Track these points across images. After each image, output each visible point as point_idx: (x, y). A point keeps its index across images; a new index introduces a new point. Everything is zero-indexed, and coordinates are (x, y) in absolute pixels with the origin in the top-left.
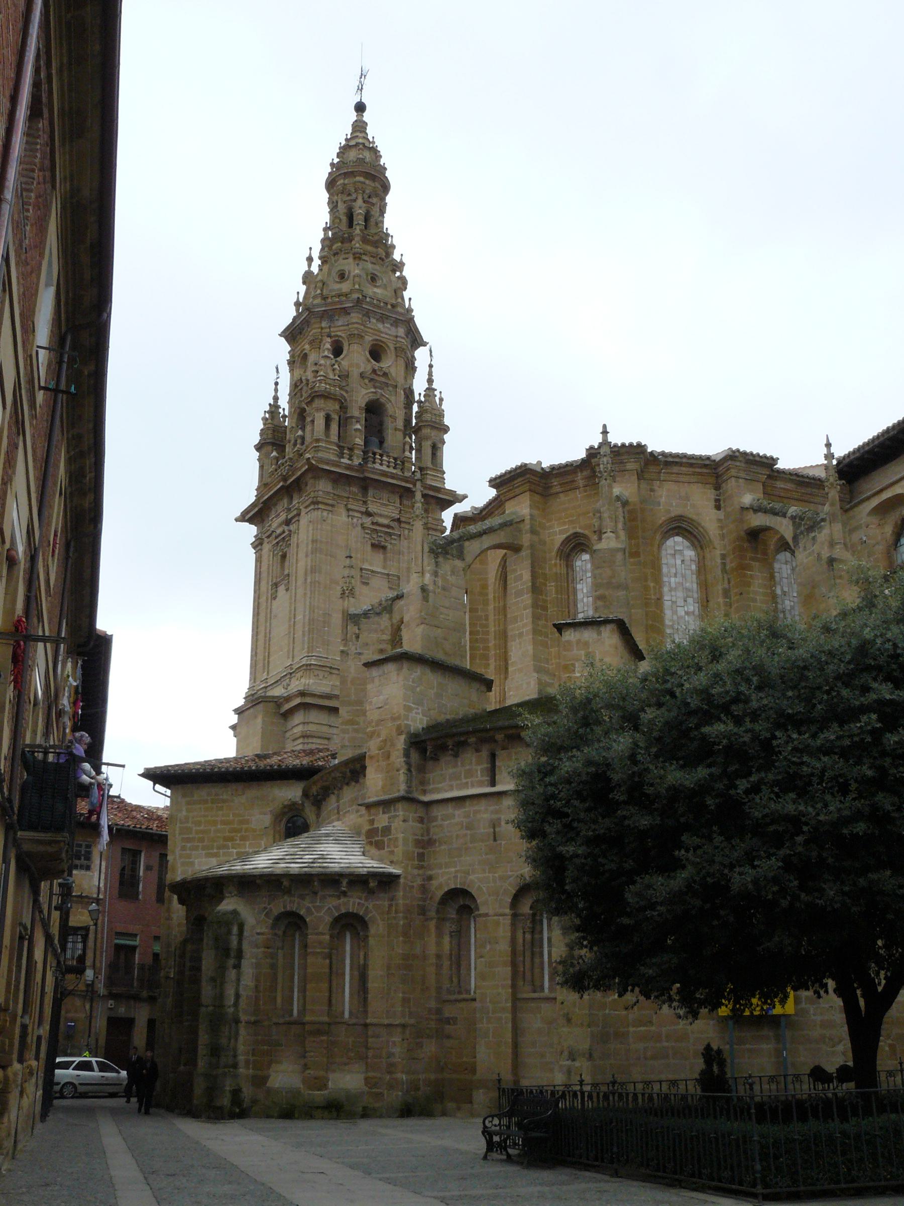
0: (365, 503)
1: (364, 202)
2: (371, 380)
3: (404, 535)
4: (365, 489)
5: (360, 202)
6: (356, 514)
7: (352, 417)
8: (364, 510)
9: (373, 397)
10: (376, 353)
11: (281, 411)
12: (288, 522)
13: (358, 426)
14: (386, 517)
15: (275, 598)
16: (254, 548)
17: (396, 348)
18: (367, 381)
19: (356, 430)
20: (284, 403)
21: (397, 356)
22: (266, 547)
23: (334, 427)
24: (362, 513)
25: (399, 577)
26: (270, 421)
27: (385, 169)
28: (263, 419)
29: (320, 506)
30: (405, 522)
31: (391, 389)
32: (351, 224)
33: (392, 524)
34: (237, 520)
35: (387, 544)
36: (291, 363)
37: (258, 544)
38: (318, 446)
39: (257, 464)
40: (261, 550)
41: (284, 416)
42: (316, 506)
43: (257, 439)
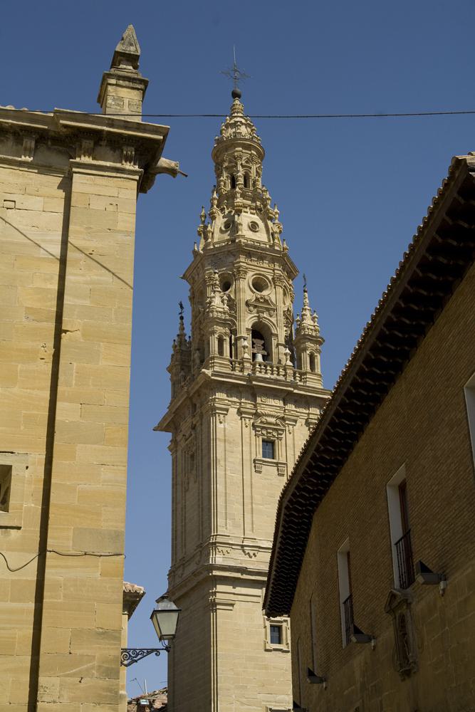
2: (255, 307)
5: (240, 168)
7: (241, 338)
8: (254, 411)
10: (258, 285)
11: (187, 338)
12: (194, 428)
13: (246, 343)
15: (187, 490)
16: (171, 451)
18: (252, 308)
19: (244, 347)
20: (188, 332)
21: (275, 286)
22: (180, 448)
23: (226, 347)
24: (252, 414)
26: (178, 348)
28: (173, 347)
30: (290, 420)
32: (234, 186)
34: (154, 430)
36: (192, 298)
38: (213, 363)
39: (170, 384)
40: (176, 451)
41: (190, 343)
43: (168, 362)
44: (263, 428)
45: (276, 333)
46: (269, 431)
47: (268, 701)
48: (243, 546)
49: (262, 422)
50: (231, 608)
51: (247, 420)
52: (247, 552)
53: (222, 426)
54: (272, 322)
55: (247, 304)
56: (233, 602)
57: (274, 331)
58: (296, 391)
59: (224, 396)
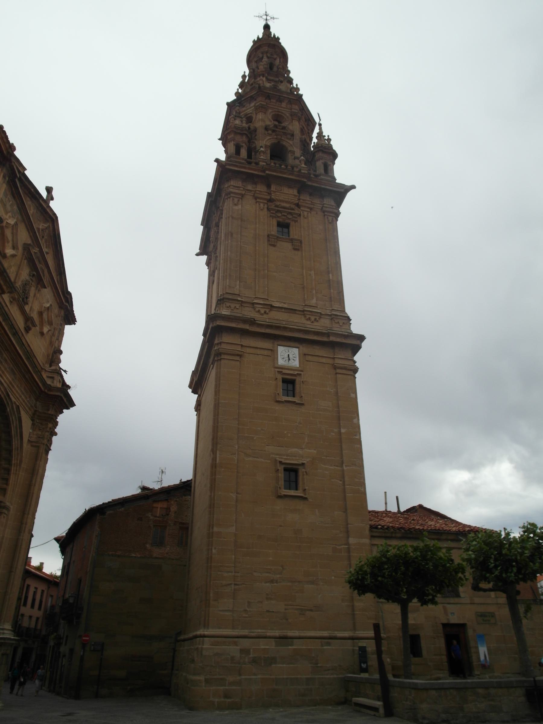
0: (270, 194)
1: (268, 57)
2: (274, 131)
3: (304, 216)
4: (269, 186)
6: (261, 201)
8: (269, 197)
9: (276, 141)
14: (287, 202)
17: (291, 115)
18: (270, 132)
25: (301, 242)
27: (278, 39)
29: (232, 195)
31: (289, 136)
33: (293, 206)
34: (197, 255)
35: (289, 221)
37: (208, 263)
42: (229, 196)
44: (278, 211)
45: (292, 149)
46: (283, 214)
47: (277, 454)
48: (253, 304)
49: (276, 206)
50: (237, 358)
51: (262, 205)
52: (257, 309)
53: (236, 208)
54: (289, 143)
55: (266, 129)
56: (240, 353)
57: (290, 148)
58: (310, 183)
59: (239, 184)
